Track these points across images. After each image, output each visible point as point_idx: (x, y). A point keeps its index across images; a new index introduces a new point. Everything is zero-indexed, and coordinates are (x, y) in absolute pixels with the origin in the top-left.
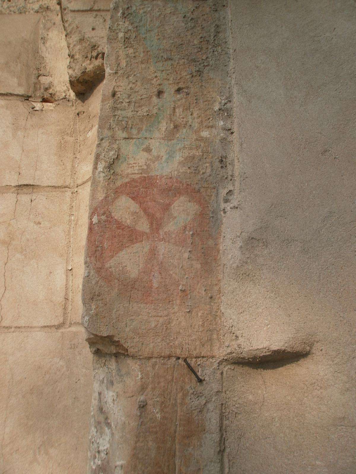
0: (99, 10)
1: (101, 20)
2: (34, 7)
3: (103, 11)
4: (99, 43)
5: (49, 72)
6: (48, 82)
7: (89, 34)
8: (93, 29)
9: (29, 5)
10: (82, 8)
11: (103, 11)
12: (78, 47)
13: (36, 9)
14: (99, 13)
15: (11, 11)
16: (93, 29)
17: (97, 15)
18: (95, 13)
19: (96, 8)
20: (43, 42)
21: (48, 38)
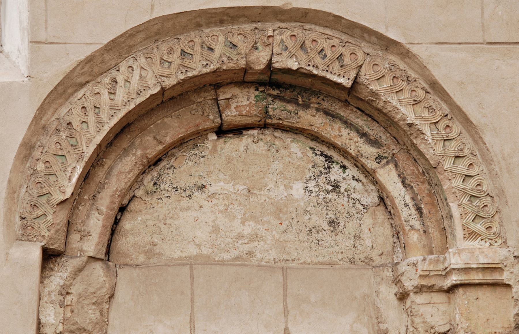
0: (435, 303)
1: (436, 310)
2: (360, 257)
3: (437, 303)
4: (436, 326)
5: (385, 320)
6: (385, 328)
7: (429, 319)
8: (432, 316)
9: (356, 255)
10: (424, 302)
11: (437, 303)
12: (422, 325)
13: (362, 259)
14: (434, 305)
15: (344, 261)
16: (432, 316)
17: (433, 306)
18: (432, 305)
19: (432, 302)
20: (376, 294)
21: (380, 291)
